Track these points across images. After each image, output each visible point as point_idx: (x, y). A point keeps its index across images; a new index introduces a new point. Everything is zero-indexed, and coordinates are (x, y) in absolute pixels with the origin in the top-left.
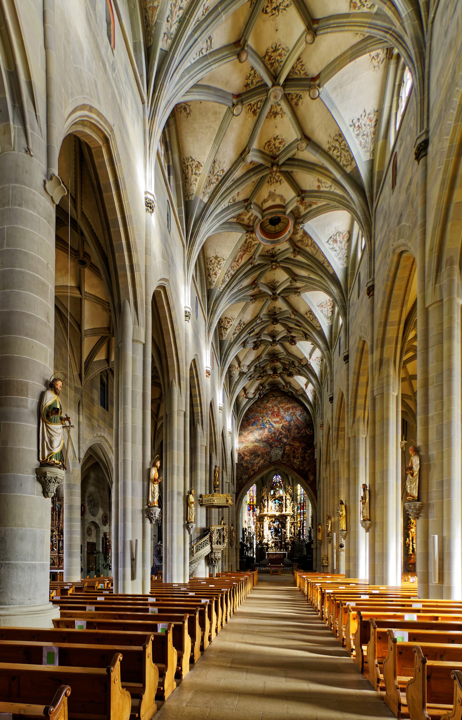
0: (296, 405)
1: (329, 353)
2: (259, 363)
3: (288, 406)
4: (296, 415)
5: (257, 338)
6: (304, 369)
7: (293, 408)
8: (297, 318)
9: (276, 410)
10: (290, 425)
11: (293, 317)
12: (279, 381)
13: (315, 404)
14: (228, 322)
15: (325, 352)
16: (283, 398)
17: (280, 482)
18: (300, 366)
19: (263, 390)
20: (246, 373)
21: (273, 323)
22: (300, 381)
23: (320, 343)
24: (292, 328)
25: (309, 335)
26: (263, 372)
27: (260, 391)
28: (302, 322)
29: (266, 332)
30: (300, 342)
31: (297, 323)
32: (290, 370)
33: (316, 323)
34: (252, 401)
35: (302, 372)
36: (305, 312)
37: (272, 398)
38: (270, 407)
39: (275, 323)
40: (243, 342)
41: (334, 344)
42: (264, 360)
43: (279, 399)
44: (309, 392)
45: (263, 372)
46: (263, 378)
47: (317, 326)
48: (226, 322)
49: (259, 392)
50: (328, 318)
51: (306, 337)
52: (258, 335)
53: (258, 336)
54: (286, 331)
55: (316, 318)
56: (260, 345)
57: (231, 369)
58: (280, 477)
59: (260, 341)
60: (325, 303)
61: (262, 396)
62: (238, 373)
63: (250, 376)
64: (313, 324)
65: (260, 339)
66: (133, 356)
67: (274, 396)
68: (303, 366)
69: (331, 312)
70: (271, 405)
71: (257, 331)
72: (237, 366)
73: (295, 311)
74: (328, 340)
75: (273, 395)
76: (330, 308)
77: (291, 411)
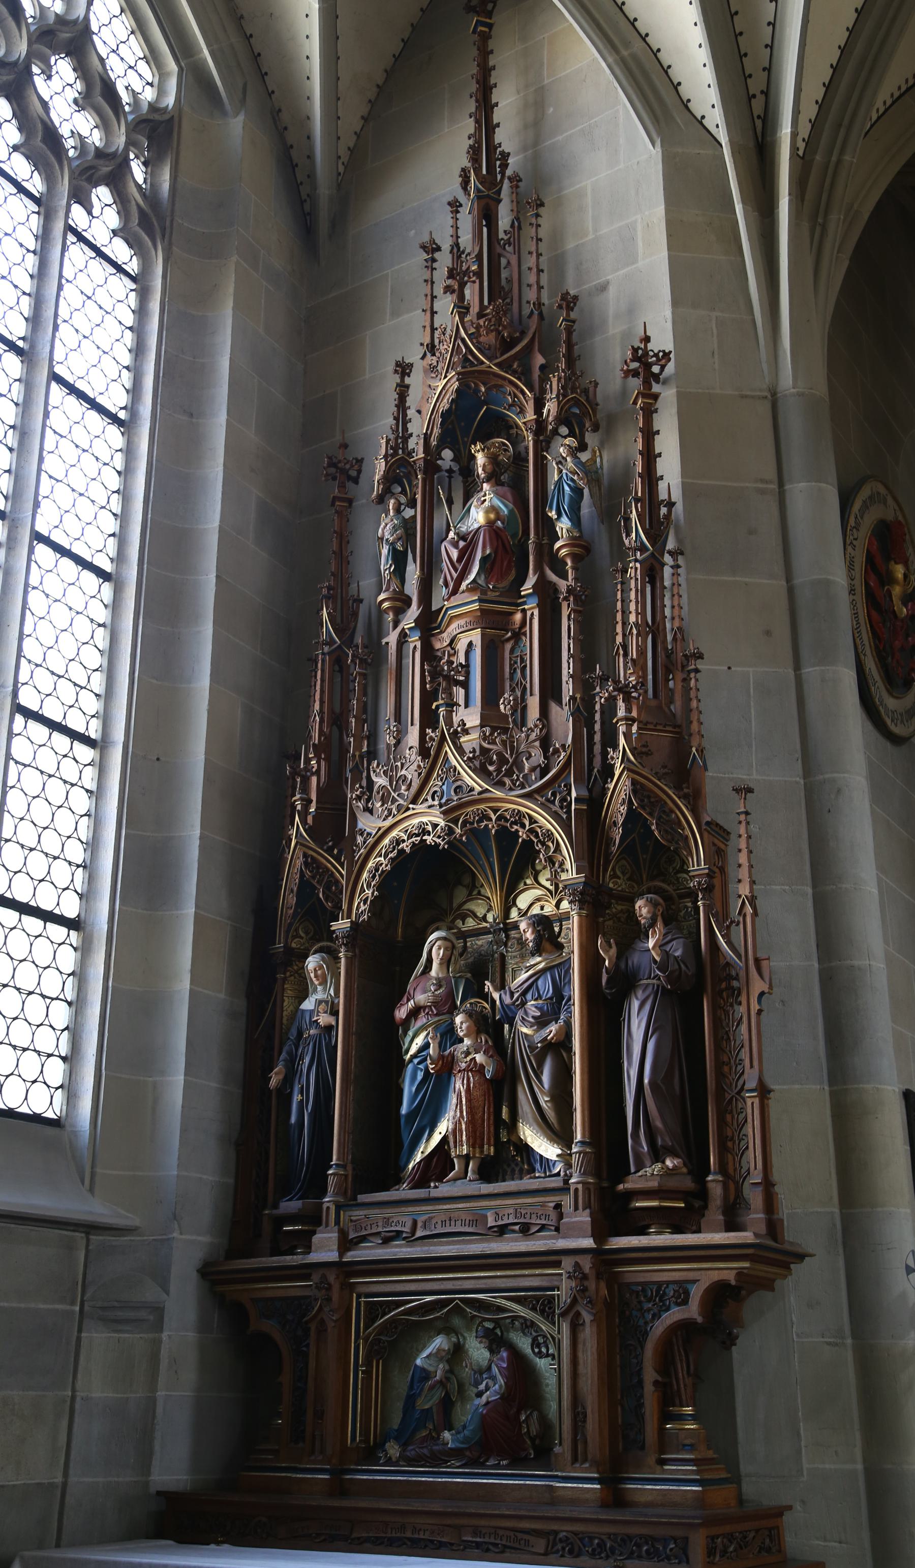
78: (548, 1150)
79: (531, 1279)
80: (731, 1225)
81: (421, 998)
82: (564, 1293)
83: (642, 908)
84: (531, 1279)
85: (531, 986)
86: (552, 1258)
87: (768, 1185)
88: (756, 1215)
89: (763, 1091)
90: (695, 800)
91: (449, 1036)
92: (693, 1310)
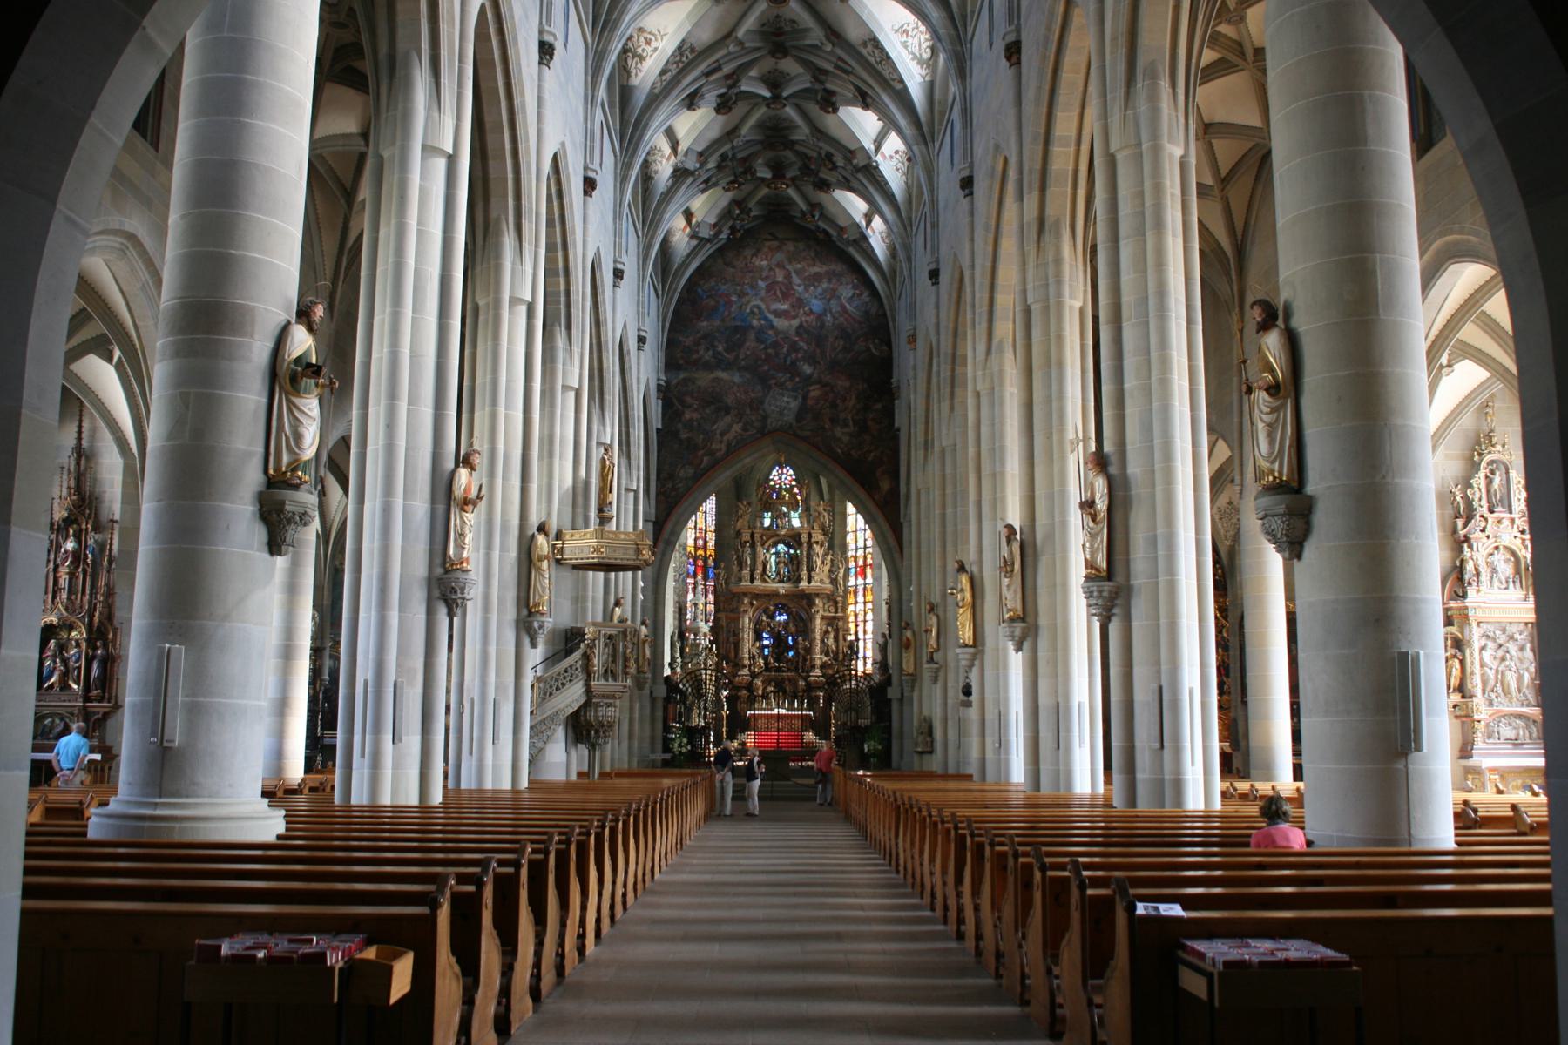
0: (838, 267)
1: (925, 150)
2: (733, 148)
3: (816, 269)
4: (839, 298)
5: (730, 87)
6: (860, 176)
7: (831, 275)
8: (839, 52)
9: (780, 279)
10: (822, 326)
11: (829, 47)
12: (790, 199)
13: (895, 272)
14: (648, 42)
15: (915, 148)
16: (801, 246)
17: (792, 487)
18: (849, 168)
19: (743, 220)
20: (692, 173)
21: (773, 54)
22: (855, 205)
23: (902, 122)
24: (825, 72)
25: (871, 97)
26: (745, 173)
27: (735, 220)
28: (853, 63)
29: (753, 73)
30: (850, 108)
31: (840, 64)
32: (821, 175)
33: (891, 70)
34: (709, 245)
35: (855, 184)
36: (860, 42)
37: (767, 244)
38: (762, 269)
39: (778, 55)
40: (688, 95)
41: (939, 130)
42: (748, 142)
43: (790, 246)
44: (877, 234)
45: (745, 173)
46: (743, 187)
47: (894, 80)
48: (642, 39)
49: (730, 223)
50: (921, 62)
51: (865, 101)
52: (734, 78)
53: (729, 82)
54: (808, 77)
55: (889, 58)
56: (735, 103)
57: (651, 158)
58: (791, 472)
59: (736, 94)
60: (911, 26)
61: (739, 235)
62: (671, 170)
63: (706, 181)
64: (883, 72)
65: (736, 91)
66: (420, 185)
67: (776, 238)
68: (858, 169)
69: (928, 50)
70: (765, 263)
71: (727, 69)
72: (667, 150)
73: (835, 34)
74: (923, 119)
75: (770, 234)
76: (927, 40)
77: (825, 285)
78: (75, 687)
79: (69, 709)
80: (109, 702)
81: (49, 654)
82: (76, 712)
83: (98, 644)
84: (69, 709)
85: (74, 655)
86: (75, 706)
87: (116, 696)
88: (113, 701)
89: (118, 679)
90: (111, 624)
91: (55, 662)
92: (100, 716)
